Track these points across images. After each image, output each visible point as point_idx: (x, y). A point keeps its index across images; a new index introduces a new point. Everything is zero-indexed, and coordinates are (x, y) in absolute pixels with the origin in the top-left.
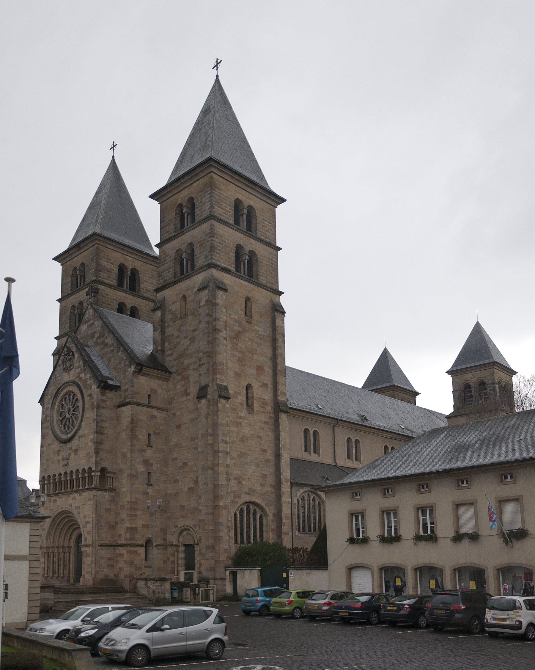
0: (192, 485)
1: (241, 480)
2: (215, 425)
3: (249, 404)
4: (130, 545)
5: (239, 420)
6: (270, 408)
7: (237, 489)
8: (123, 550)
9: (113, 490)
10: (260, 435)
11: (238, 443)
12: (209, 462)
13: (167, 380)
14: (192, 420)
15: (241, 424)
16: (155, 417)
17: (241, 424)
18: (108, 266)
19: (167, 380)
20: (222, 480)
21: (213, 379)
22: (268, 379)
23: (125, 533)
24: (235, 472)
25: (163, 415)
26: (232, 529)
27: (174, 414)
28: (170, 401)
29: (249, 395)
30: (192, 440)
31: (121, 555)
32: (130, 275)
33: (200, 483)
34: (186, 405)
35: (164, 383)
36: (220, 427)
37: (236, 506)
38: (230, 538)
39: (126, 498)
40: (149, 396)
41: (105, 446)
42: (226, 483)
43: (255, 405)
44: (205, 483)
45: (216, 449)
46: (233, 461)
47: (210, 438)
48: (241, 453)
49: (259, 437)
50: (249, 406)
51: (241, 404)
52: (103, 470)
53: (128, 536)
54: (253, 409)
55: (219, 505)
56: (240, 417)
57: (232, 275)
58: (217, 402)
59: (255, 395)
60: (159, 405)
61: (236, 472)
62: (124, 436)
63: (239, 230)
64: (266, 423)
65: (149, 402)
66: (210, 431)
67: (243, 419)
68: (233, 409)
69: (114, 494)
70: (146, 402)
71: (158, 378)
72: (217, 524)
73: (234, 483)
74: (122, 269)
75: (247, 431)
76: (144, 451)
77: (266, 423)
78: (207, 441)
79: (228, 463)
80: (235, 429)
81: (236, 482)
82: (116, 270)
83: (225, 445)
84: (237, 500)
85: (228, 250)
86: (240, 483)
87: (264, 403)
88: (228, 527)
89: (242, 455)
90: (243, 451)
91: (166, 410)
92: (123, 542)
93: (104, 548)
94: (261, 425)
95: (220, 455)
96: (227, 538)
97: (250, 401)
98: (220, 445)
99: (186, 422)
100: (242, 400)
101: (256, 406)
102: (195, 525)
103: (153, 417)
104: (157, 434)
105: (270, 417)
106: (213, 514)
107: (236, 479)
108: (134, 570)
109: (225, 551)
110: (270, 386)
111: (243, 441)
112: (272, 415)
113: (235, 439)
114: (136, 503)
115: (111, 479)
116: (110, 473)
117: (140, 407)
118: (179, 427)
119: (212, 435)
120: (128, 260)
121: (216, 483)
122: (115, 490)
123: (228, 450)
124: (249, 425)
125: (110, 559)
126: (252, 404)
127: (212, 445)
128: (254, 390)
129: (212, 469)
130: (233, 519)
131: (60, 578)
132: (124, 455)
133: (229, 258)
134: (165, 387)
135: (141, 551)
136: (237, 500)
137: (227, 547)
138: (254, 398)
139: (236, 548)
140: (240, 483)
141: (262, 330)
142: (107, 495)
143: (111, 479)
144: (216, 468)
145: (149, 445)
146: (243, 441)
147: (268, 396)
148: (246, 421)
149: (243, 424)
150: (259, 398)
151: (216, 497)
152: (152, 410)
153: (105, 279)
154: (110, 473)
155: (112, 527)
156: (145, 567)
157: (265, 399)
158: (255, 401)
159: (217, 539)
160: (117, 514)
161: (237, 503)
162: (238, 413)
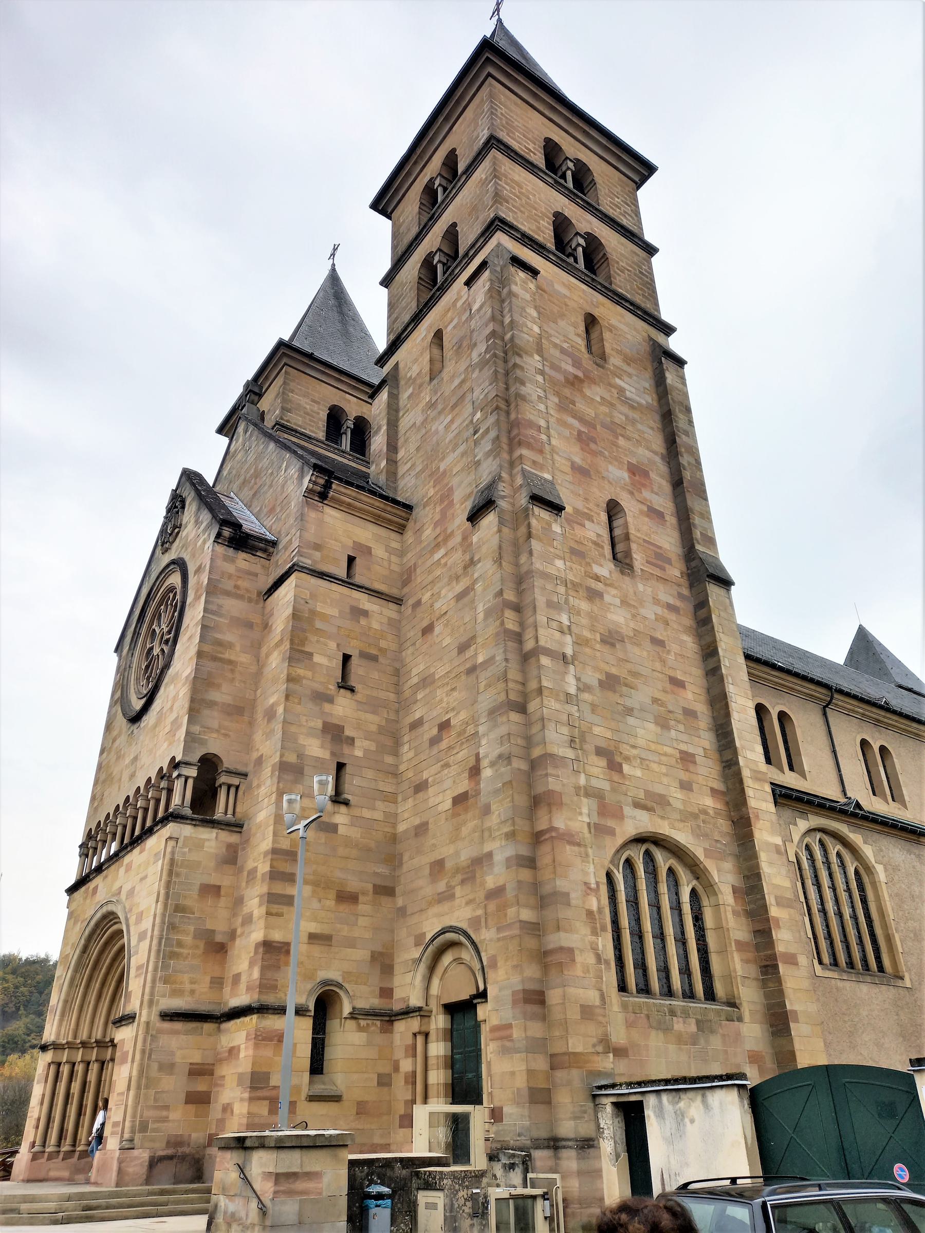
0: (464, 785)
1: (618, 759)
2: (521, 580)
3: (619, 556)
4: (261, 1009)
5: (599, 586)
6: (677, 573)
7: (606, 786)
8: (238, 1034)
9: (236, 826)
10: (658, 635)
11: (598, 646)
12: (511, 685)
13: (401, 529)
14: (459, 597)
15: (600, 595)
16: (365, 613)
17: (600, 595)
18: (304, 402)
19: (401, 529)
20: (556, 740)
21: (512, 464)
22: (664, 502)
23: (252, 964)
24: (597, 730)
25: (390, 611)
26: (604, 929)
27: (418, 603)
28: (407, 576)
29: (617, 532)
30: (463, 648)
31: (233, 1052)
32: (352, 427)
33: (485, 763)
34: (446, 564)
35: (394, 535)
36: (538, 582)
37: (612, 845)
38: (598, 958)
39: (262, 842)
40: (351, 560)
41: (222, 695)
42: (570, 754)
43: (635, 556)
44: (500, 756)
45: (529, 645)
46: (586, 696)
47: (509, 614)
48: (609, 676)
49: (656, 642)
50: (621, 559)
51: (595, 543)
52: (209, 765)
53: (256, 974)
54: (630, 567)
55: (552, 829)
56: (597, 578)
57: (547, 258)
58: (526, 513)
59: (632, 531)
60: (378, 586)
61: (601, 732)
62: (276, 662)
63: (558, 186)
64: (670, 607)
65: (349, 575)
66: (510, 596)
67: (606, 585)
68: (573, 551)
69: (233, 838)
70: (342, 572)
71: (378, 520)
72: (544, 898)
73: (597, 766)
74: (335, 417)
75: (618, 618)
76: (330, 700)
77: (670, 607)
78: (502, 623)
79: (572, 690)
80: (584, 605)
81: (603, 762)
82: (324, 415)
83: (557, 635)
84: (610, 823)
85: (536, 215)
86: (614, 766)
87: (659, 558)
88: (590, 913)
89: (610, 683)
90: (614, 671)
91: (398, 601)
92: (240, 999)
93: (178, 1026)
94: (659, 610)
95: (545, 661)
96: (591, 959)
97: (620, 547)
98: (541, 631)
99: (444, 609)
100: (598, 535)
101: (638, 559)
102: (475, 922)
103: (358, 613)
104: (374, 658)
105: (680, 596)
106: (530, 863)
107: (600, 752)
108: (265, 1112)
109: (587, 1012)
110: (671, 520)
111: (613, 645)
112: (686, 592)
113: (587, 634)
114: (291, 855)
115: (233, 790)
116: (229, 772)
117: (320, 582)
118: (428, 630)
119: (517, 609)
120: (349, 401)
121: (537, 752)
122: (241, 826)
123: (569, 651)
124: (624, 603)
125: (201, 1071)
126: (628, 553)
127: (518, 638)
128: (630, 519)
129: (522, 709)
130: (604, 889)
131: (77, 1154)
132: (270, 714)
133: (539, 228)
134: (395, 545)
135: (300, 1032)
136: (610, 823)
137: (592, 997)
138: (631, 537)
139: (624, 1006)
140: (614, 766)
141: (633, 390)
142: (211, 840)
143: (233, 790)
144: (532, 706)
145: (345, 685)
146: (613, 645)
147: (668, 540)
148: (614, 592)
149: (607, 598)
150: (645, 541)
151: (538, 801)
152: (356, 594)
153: (300, 427)
154: (229, 772)
155: (218, 949)
156: (312, 1098)
157: (660, 548)
158: (634, 546)
159: (549, 961)
160: (239, 901)
161: (612, 832)
162: (589, 564)
